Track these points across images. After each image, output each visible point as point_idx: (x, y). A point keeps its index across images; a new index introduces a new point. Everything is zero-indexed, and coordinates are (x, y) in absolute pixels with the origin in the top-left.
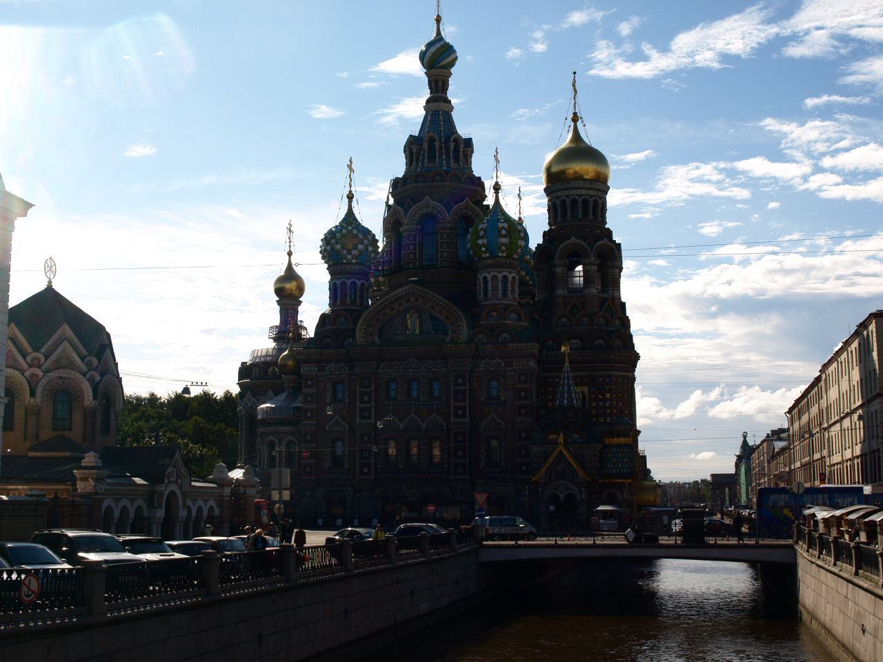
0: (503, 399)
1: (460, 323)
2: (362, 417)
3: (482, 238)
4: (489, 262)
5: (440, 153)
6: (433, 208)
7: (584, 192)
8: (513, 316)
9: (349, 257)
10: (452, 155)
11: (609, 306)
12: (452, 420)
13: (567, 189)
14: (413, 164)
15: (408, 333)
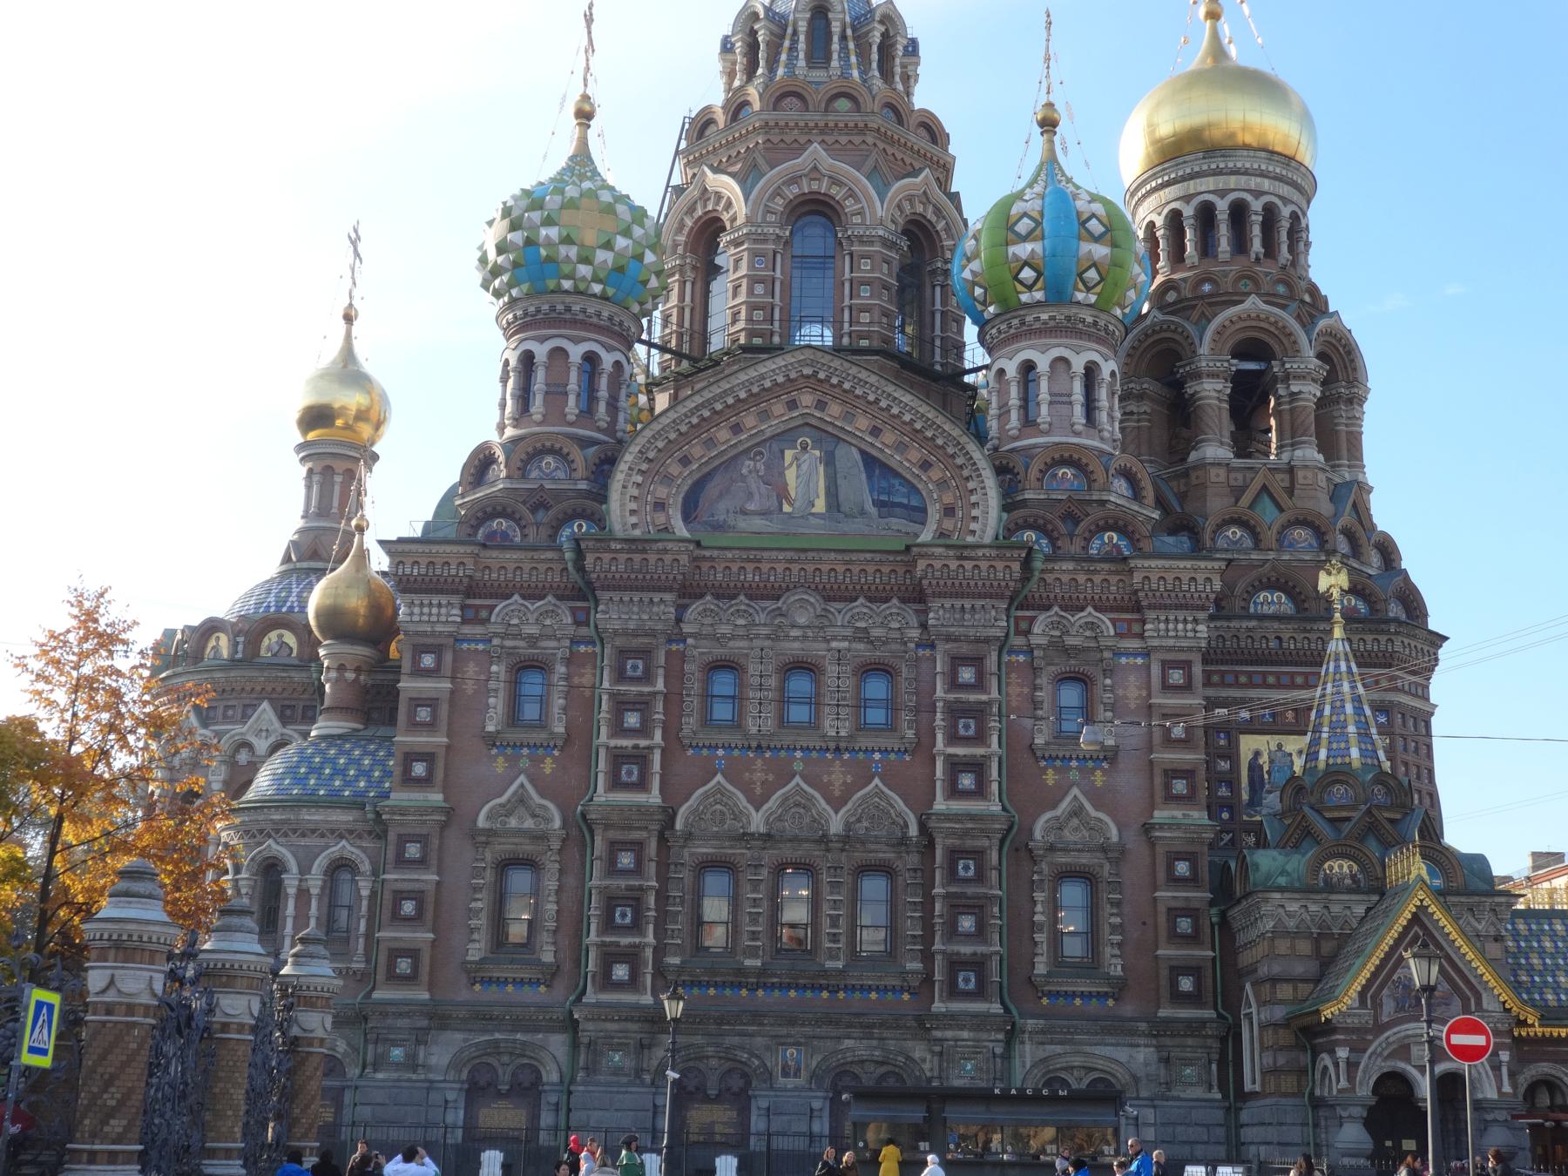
0: (1110, 742)
1: (971, 485)
2: (616, 784)
3: (1024, 239)
4: (1044, 317)
5: (844, 48)
6: (835, 181)
7: (1266, 184)
8: (1121, 485)
9: (584, 270)
10: (875, 56)
11: (1355, 505)
12: (940, 805)
13: (1218, 172)
14: (760, 71)
15: (786, 508)
